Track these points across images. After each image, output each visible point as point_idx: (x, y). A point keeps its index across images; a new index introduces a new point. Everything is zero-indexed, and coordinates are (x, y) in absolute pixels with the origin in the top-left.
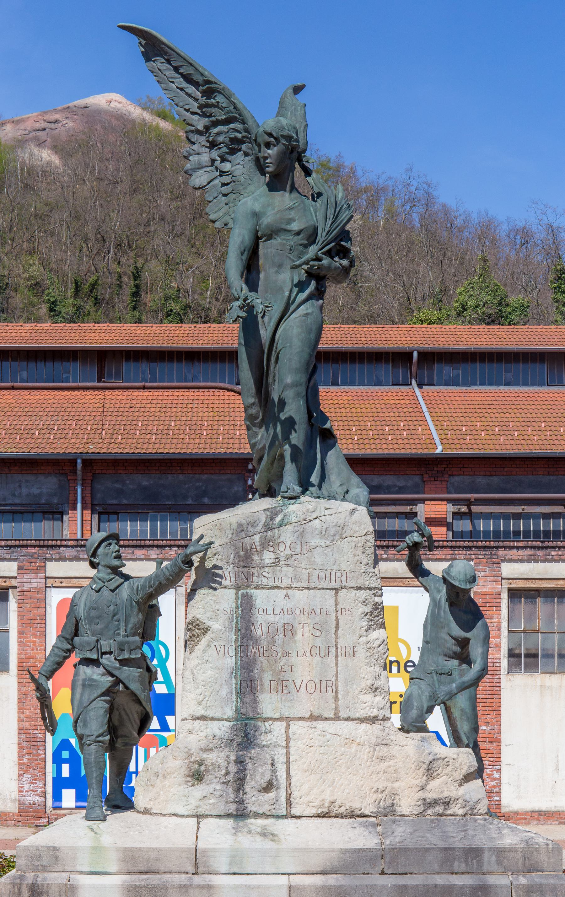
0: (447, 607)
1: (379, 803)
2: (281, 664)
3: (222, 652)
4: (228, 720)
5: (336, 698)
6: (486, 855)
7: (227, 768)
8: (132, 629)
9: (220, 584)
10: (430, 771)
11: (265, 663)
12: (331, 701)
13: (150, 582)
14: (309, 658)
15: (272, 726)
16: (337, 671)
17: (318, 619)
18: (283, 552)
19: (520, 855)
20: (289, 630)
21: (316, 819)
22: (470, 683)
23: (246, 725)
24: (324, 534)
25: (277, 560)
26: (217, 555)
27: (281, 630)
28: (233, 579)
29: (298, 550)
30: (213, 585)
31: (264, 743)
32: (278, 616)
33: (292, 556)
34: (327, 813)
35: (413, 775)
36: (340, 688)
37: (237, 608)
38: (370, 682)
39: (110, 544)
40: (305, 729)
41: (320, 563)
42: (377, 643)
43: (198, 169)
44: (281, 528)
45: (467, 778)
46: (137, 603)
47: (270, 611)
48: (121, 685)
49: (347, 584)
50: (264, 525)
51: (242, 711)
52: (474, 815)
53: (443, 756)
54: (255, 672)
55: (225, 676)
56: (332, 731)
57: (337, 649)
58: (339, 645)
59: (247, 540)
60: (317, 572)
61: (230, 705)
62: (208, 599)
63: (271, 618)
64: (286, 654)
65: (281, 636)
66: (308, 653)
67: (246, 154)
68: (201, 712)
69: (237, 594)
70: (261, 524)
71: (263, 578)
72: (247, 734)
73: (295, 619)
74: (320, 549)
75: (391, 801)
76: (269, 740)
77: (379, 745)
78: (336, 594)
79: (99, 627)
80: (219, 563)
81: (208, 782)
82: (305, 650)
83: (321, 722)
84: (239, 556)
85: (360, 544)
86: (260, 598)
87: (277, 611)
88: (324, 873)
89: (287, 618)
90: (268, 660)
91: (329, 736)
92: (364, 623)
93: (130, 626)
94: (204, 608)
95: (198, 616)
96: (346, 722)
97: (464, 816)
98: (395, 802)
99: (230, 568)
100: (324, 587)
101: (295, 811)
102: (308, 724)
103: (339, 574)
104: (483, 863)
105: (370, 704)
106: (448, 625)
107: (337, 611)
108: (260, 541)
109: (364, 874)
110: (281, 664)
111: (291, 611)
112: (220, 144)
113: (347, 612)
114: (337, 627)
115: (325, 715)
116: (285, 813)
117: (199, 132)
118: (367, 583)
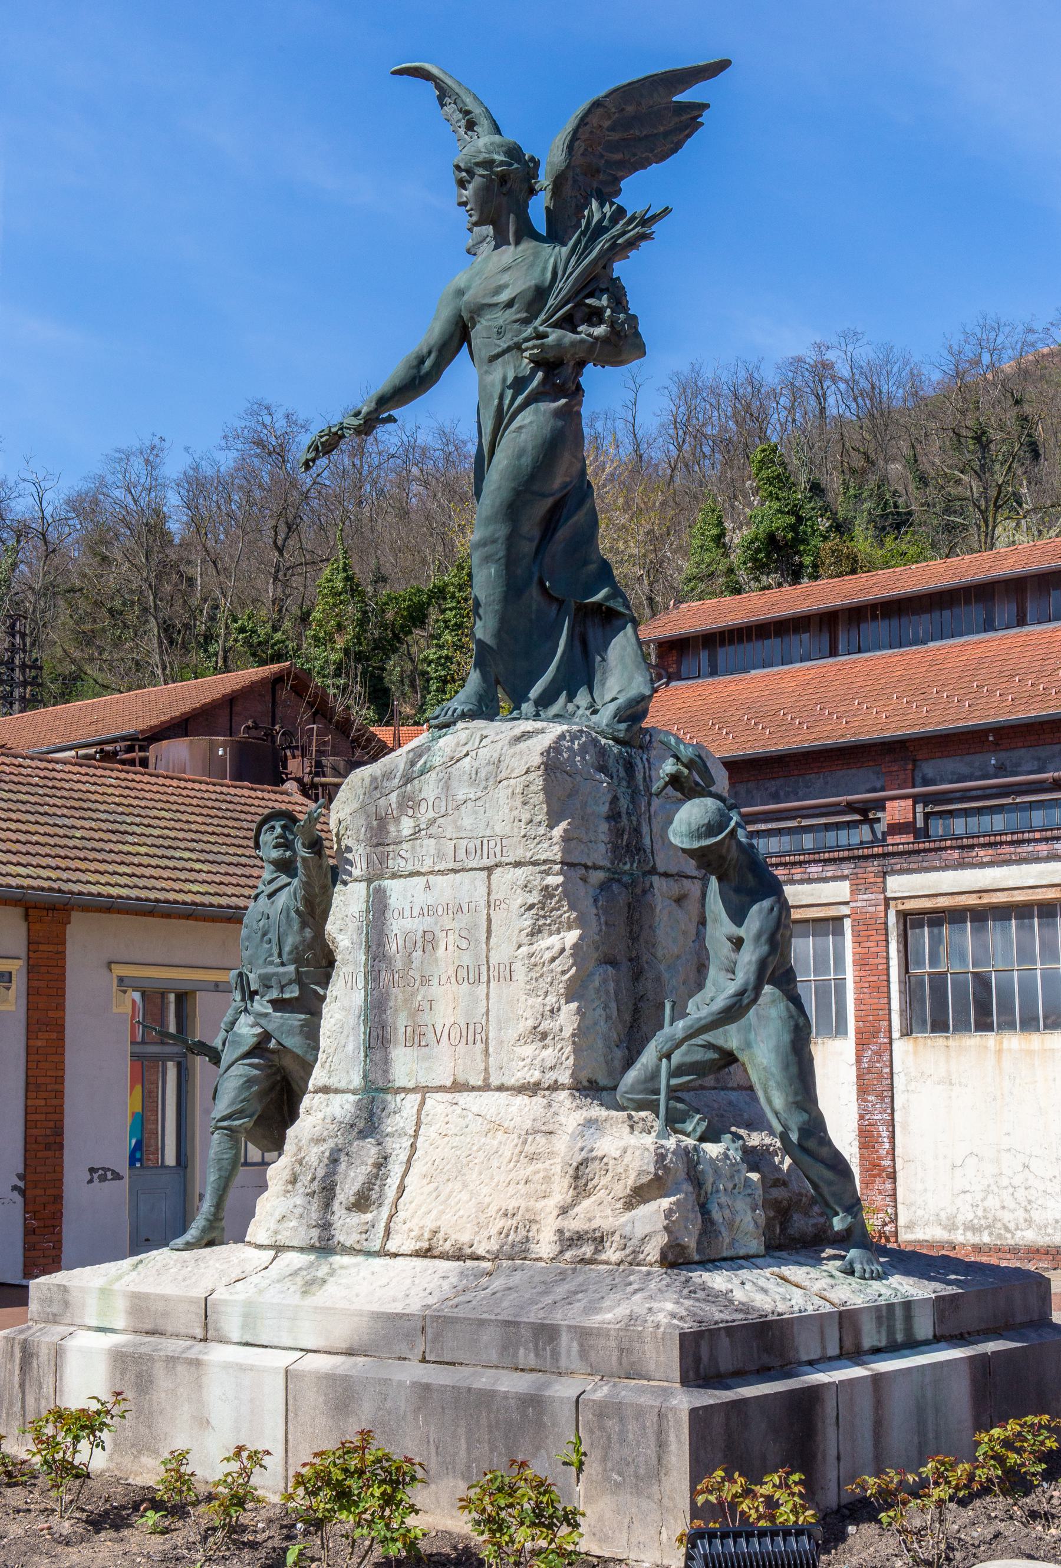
1: (507, 1236)
2: (419, 998)
4: (354, 1092)
6: (564, 1337)
8: (290, 953)
9: (350, 874)
10: (581, 1178)
11: (400, 997)
17: (463, 920)
18: (426, 814)
19: (613, 1344)
20: (429, 941)
22: (709, 1019)
24: (474, 778)
28: (364, 866)
29: (443, 809)
31: (389, 1129)
32: (416, 920)
33: (435, 821)
34: (429, 1250)
37: (368, 911)
38: (530, 1023)
39: (273, 827)
40: (442, 1106)
42: (548, 955)
45: (639, 1195)
46: (297, 912)
47: (407, 914)
48: (273, 1041)
50: (403, 776)
52: (638, 1265)
53: (600, 1154)
55: (352, 1021)
56: (475, 1109)
58: (491, 961)
59: (382, 802)
60: (465, 841)
63: (408, 924)
64: (425, 981)
65: (420, 952)
66: (453, 979)
70: (399, 775)
71: (400, 860)
72: (371, 1114)
73: (436, 923)
74: (470, 804)
75: (524, 1233)
77: (536, 1132)
78: (489, 877)
83: (465, 1094)
84: (372, 828)
85: (519, 790)
87: (415, 913)
88: (350, 1353)
92: (527, 923)
93: (287, 949)
96: (497, 1094)
97: (619, 1265)
98: (530, 1234)
100: (475, 866)
101: (392, 1247)
102: (448, 1096)
103: (492, 843)
104: (559, 1353)
105: (528, 1061)
109: (399, 1358)
110: (419, 998)
111: (429, 910)
114: (489, 931)
115: (472, 1082)
116: (377, 1248)
118: (529, 854)
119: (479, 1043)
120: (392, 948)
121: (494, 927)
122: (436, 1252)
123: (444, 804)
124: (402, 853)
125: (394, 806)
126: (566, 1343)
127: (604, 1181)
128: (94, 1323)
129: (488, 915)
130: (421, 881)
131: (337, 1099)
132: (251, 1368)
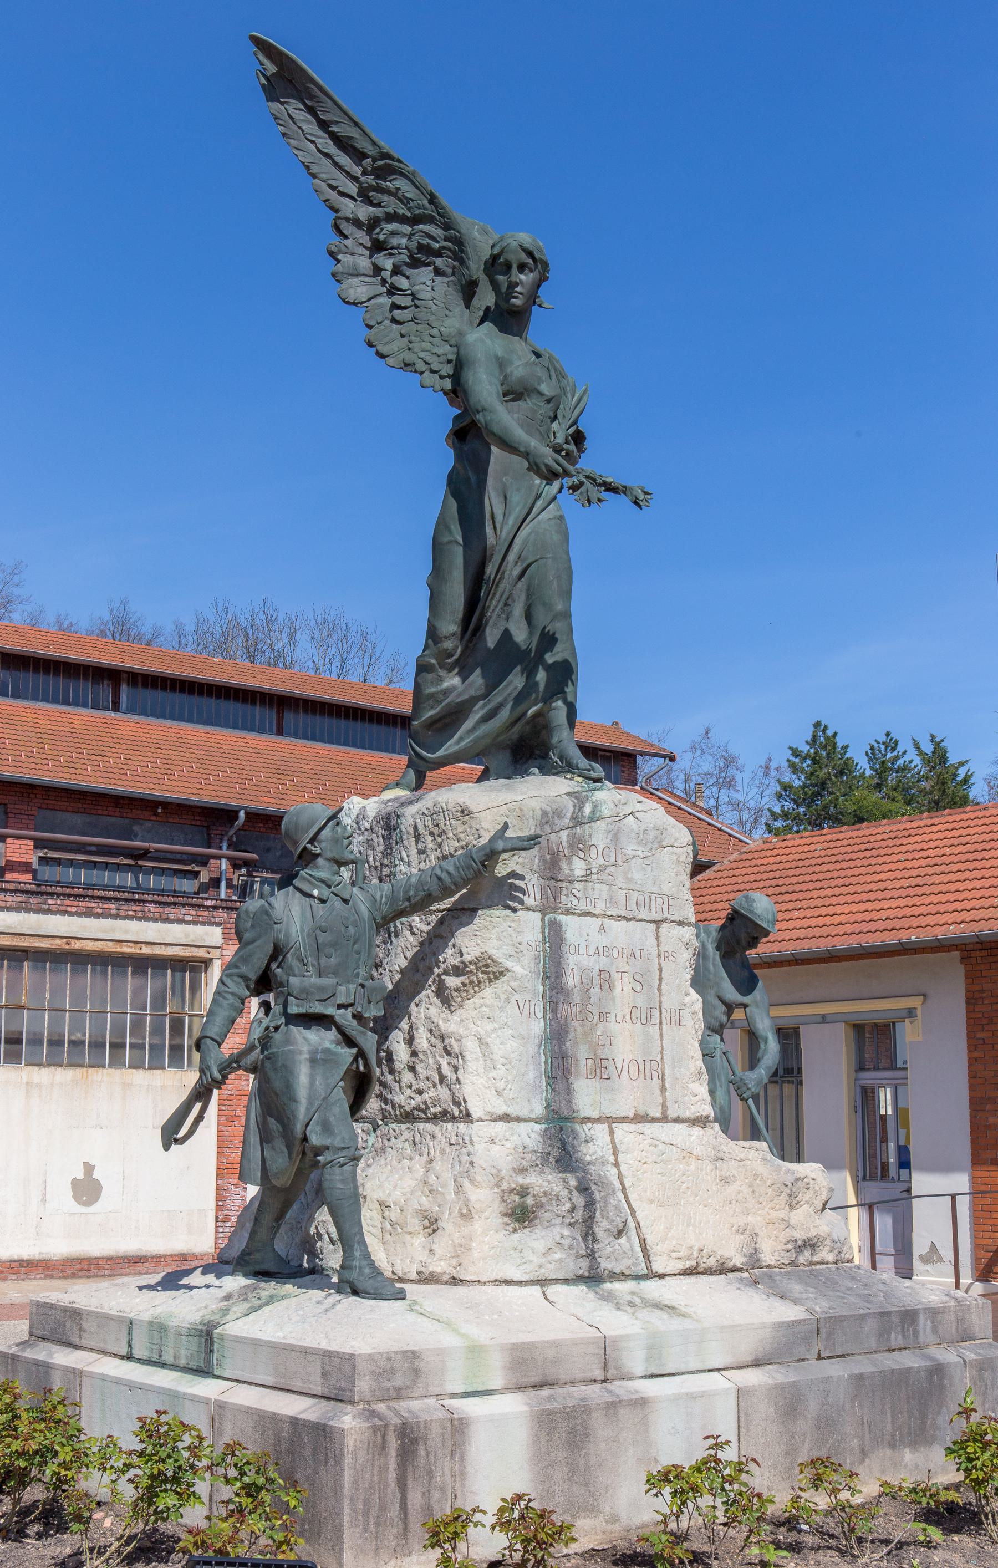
0: (718, 958)
2: (599, 1033)
3: (526, 1012)
4: (537, 1121)
5: (663, 1089)
6: (922, 1318)
7: (570, 1199)
9: (521, 902)
11: (579, 1030)
12: (658, 1092)
13: (406, 892)
14: (628, 1026)
15: (592, 1131)
16: (662, 1046)
19: (953, 1317)
20: (606, 980)
21: (682, 1277)
23: (561, 1129)
24: (640, 838)
25: (588, 872)
27: (596, 981)
28: (538, 897)
29: (613, 859)
35: (772, 1205)
36: (667, 1072)
40: (632, 1136)
41: (639, 882)
43: (352, 275)
44: (593, 824)
47: (583, 951)
49: (669, 916)
51: (554, 1106)
54: (568, 1043)
55: (532, 1049)
57: (661, 1011)
60: (636, 894)
61: (538, 1097)
62: (505, 925)
63: (586, 961)
64: (603, 1017)
65: (597, 989)
66: (628, 1017)
67: (438, 272)
68: (502, 1109)
69: (543, 920)
70: (569, 815)
71: (572, 898)
72: (564, 1144)
73: (612, 964)
76: (594, 1154)
78: (658, 928)
79: (333, 961)
80: (519, 870)
81: (546, 1224)
82: (624, 1012)
86: (572, 927)
87: (591, 951)
88: (756, 1364)
89: (603, 962)
90: (583, 1026)
91: (661, 1146)
94: (499, 939)
95: (492, 952)
99: (534, 881)
101: (658, 1267)
102: (632, 1127)
103: (659, 900)
104: (918, 1332)
106: (718, 984)
107: (659, 956)
108: (568, 841)
109: (799, 1360)
112: (391, 248)
113: (671, 958)
114: (660, 980)
117: (357, 223)
119: (655, 1078)
120: (571, 980)
121: (664, 975)
122: (700, 1269)
123: (613, 854)
124: (574, 891)
125: (565, 844)
126: (924, 1323)
127: (806, 1198)
128: (460, 1389)
129: (660, 964)
130: (596, 922)
131: (523, 1128)
132: (702, 1395)
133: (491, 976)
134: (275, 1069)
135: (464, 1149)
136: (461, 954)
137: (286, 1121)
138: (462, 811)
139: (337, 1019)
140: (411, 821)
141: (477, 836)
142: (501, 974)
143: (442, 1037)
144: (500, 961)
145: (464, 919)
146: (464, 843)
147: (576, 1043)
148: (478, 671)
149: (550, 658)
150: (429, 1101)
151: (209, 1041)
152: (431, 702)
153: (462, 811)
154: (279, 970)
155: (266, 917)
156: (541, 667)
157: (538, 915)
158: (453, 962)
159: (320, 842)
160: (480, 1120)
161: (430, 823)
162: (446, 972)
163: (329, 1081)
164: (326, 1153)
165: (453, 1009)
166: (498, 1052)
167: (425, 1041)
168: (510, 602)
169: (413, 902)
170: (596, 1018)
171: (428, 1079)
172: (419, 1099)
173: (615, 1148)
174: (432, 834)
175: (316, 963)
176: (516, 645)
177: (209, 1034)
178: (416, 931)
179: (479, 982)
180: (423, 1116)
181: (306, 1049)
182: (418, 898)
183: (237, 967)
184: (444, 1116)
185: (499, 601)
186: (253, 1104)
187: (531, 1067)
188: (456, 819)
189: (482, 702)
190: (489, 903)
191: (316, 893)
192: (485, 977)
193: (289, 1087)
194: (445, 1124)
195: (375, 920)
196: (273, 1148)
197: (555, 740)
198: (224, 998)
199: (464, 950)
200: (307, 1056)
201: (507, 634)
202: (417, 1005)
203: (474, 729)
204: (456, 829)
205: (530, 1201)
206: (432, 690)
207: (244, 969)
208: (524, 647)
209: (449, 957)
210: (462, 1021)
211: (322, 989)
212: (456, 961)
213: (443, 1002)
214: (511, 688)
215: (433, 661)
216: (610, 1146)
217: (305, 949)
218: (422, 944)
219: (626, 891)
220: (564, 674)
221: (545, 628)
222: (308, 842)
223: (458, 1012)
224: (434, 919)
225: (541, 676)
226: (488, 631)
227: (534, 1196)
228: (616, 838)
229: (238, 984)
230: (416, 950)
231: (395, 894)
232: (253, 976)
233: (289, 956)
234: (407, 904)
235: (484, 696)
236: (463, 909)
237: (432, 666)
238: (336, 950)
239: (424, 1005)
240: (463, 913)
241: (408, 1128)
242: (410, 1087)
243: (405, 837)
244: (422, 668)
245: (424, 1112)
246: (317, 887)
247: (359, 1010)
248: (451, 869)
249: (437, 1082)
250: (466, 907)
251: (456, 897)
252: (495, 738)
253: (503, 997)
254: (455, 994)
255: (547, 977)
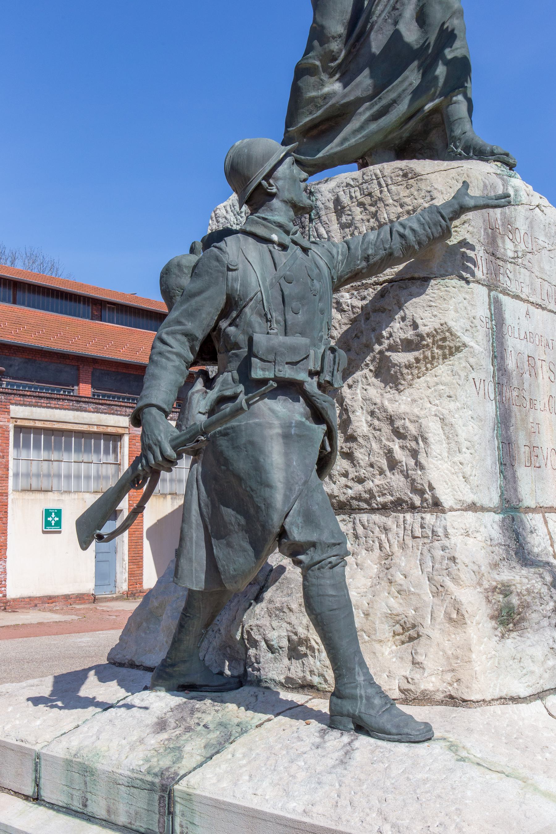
2: (531, 420)
3: (481, 392)
4: (494, 510)
7: (552, 597)
9: (473, 274)
11: (518, 414)
14: (547, 414)
15: (533, 521)
26: (466, 225)
27: (526, 367)
30: (464, 274)
41: (548, 273)
54: (512, 428)
66: (547, 406)
68: (470, 498)
69: (489, 295)
79: (301, 317)
81: (536, 627)
90: (520, 411)
94: (456, 311)
95: (451, 324)
99: (481, 253)
108: (501, 219)
120: (511, 363)
125: (499, 222)
130: (524, 306)
133: (447, 351)
134: (236, 448)
135: (436, 543)
136: (415, 326)
137: (252, 511)
138: (405, 175)
139: (307, 387)
140: (330, 196)
141: (428, 198)
142: (458, 349)
143: (391, 420)
144: (459, 334)
145: (414, 289)
146: (410, 208)
147: (517, 429)
148: (366, 72)
149: (449, 54)
150: (375, 490)
151: (154, 411)
152: (310, 107)
153: (405, 175)
154: (232, 329)
155: (216, 263)
156: (440, 62)
157: (485, 290)
158: (403, 336)
159: (277, 179)
160: (452, 509)
161: (358, 194)
162: (391, 348)
163: (307, 461)
164: (311, 552)
165: (401, 388)
166: (463, 434)
167: (365, 425)
168: (398, 6)
169: (372, 261)
170: (528, 403)
171: (372, 466)
172: (359, 488)
173: (551, 538)
174: (361, 204)
175: (280, 318)
176: (408, 46)
177: (154, 402)
178: (346, 308)
179: (433, 358)
180: (365, 506)
181: (276, 422)
182: (378, 257)
183: (179, 323)
184: (398, 505)
185: (386, 6)
186: (195, 492)
187: (489, 452)
188: (397, 184)
189: (368, 104)
190: (443, 272)
191: (275, 237)
192: (440, 352)
193: (259, 470)
194: (401, 516)
195: (332, 278)
196: (229, 545)
197: (457, 132)
198: (168, 359)
199: (419, 322)
200: (278, 431)
201: (397, 36)
202: (350, 387)
203: (362, 128)
204: (398, 194)
205: (515, 600)
206: (313, 94)
207: (189, 326)
208: (416, 47)
209: (398, 329)
210: (414, 401)
211: (293, 349)
212: (410, 334)
213: (386, 382)
214: (406, 84)
215: (318, 63)
216: (548, 537)
217: (268, 302)
218: (353, 321)
219: (540, 280)
220: (461, 70)
221: (443, 24)
222: (264, 179)
223: (407, 391)
224: (370, 293)
225: (441, 70)
226: (373, 35)
227: (518, 594)
228: (531, 226)
229: (182, 343)
230: (345, 328)
231: (353, 251)
232: (200, 335)
233: (247, 310)
234: (364, 264)
235: (370, 98)
236: (413, 279)
237: (315, 67)
238: (303, 305)
239: (360, 385)
240: (414, 282)
241: (344, 520)
242: (346, 475)
243: (322, 213)
244: (302, 71)
245: (367, 501)
246: (273, 231)
247: (328, 378)
248: (416, 226)
249: (385, 467)
250: (416, 275)
251: (401, 267)
252: (386, 136)
253: (463, 374)
254: (405, 371)
255: (495, 357)
